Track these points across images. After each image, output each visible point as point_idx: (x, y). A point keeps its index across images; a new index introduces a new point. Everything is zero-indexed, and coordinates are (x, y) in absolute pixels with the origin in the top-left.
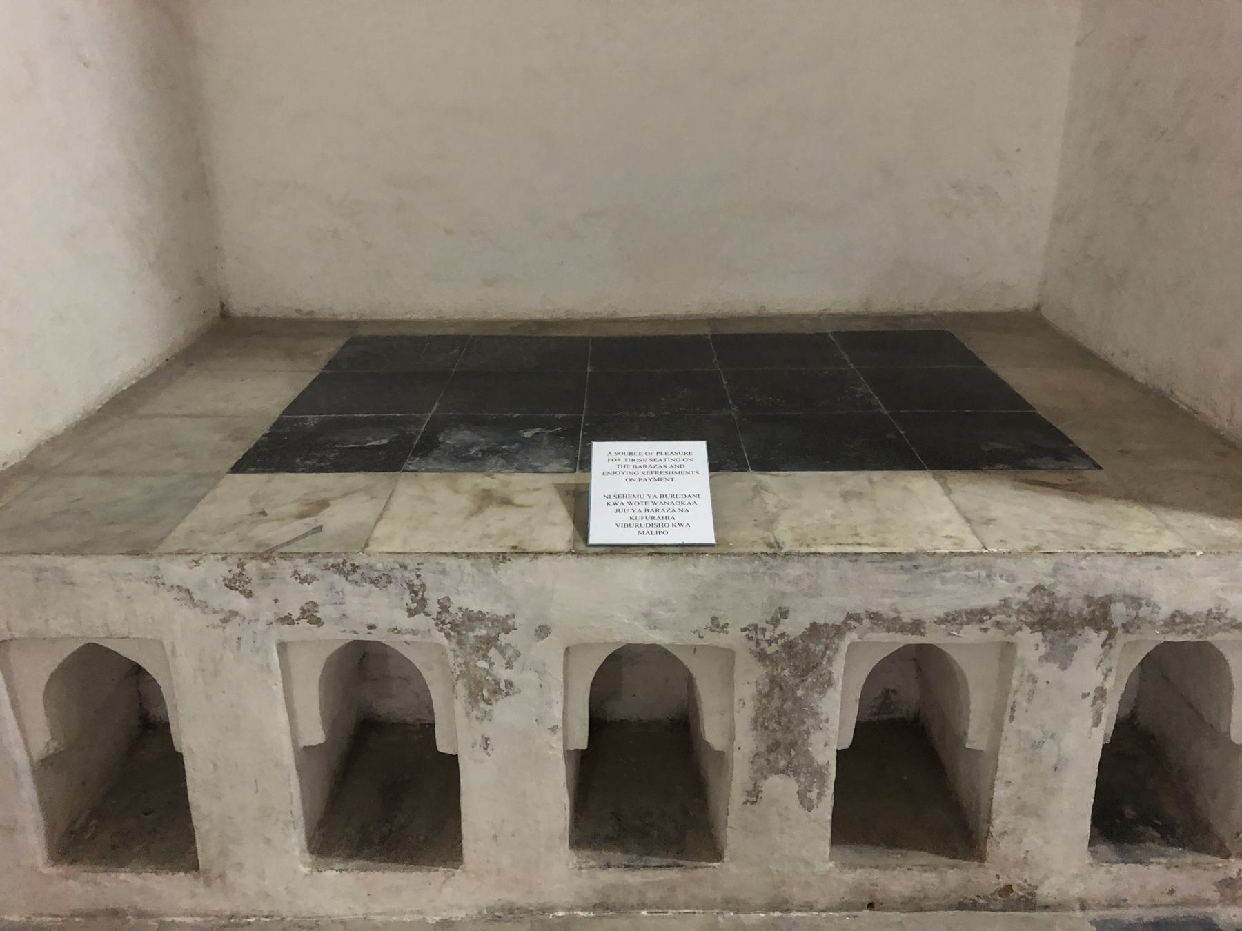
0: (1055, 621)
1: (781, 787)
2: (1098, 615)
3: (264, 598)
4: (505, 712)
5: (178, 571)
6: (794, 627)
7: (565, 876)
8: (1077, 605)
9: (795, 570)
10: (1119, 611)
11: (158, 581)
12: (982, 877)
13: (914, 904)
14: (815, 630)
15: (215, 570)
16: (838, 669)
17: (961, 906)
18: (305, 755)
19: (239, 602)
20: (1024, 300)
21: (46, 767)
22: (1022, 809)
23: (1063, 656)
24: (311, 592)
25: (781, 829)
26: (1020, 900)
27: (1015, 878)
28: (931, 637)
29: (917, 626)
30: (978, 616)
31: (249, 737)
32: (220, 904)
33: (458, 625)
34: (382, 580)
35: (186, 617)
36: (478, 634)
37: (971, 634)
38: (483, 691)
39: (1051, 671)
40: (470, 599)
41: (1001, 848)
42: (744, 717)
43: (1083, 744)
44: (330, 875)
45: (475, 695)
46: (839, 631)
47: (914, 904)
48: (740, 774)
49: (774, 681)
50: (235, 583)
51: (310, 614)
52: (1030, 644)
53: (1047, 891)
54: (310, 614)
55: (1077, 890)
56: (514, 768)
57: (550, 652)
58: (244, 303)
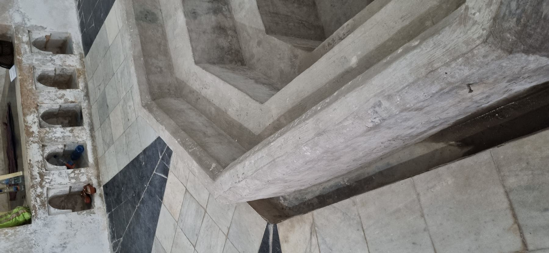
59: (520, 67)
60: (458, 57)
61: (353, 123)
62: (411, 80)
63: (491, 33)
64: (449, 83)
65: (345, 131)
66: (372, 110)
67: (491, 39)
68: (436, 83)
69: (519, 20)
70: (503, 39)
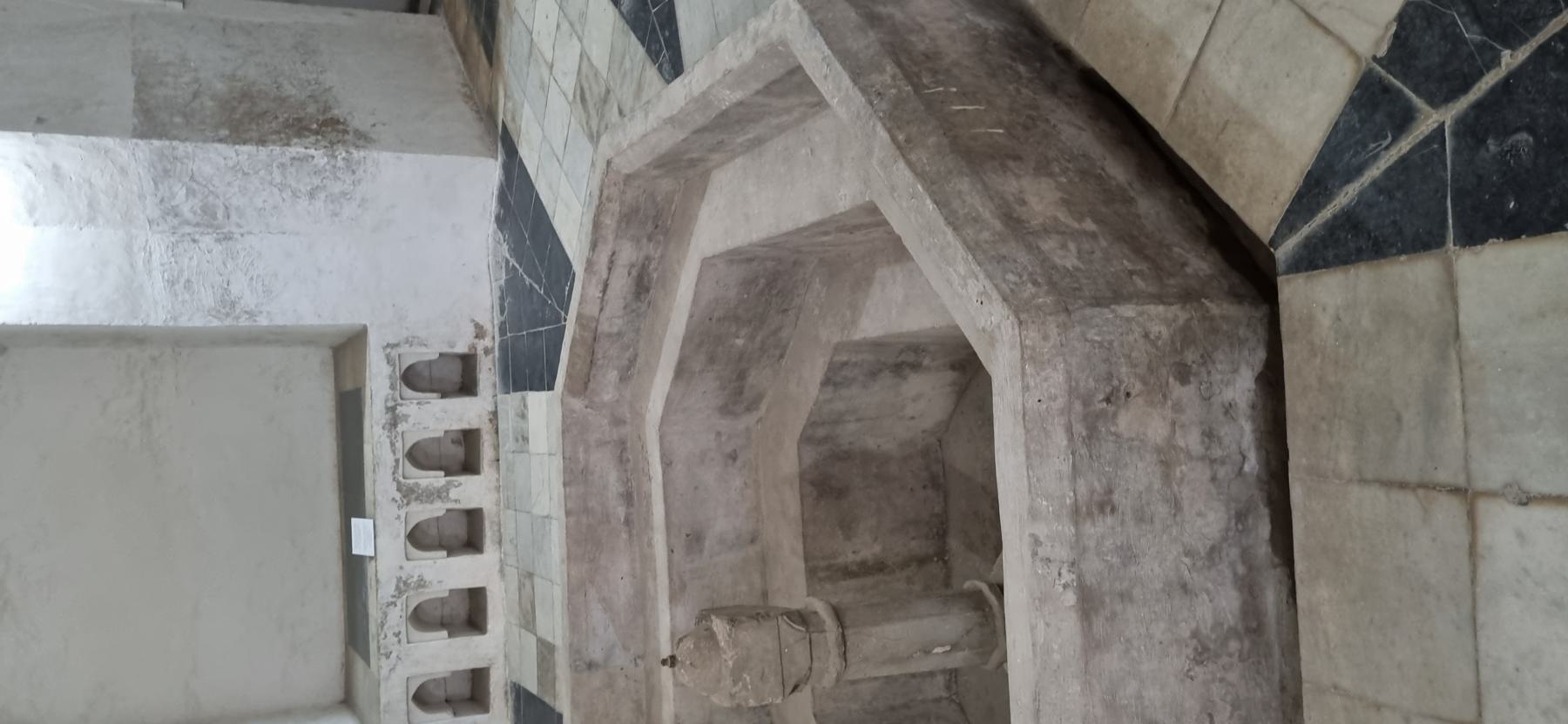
1: (453, 494)
2: (392, 409)
3: (392, 648)
4: (427, 578)
5: (384, 672)
6: (398, 496)
7: (490, 555)
8: (389, 416)
9: (379, 497)
10: (390, 404)
11: (387, 678)
13: (497, 447)
14: (399, 490)
15: (384, 661)
16: (411, 482)
18: (450, 636)
19: (394, 655)
21: (455, 714)
22: (461, 420)
23: (406, 417)
24: (390, 635)
25: (471, 491)
27: (486, 418)
28: (400, 455)
29: (397, 461)
30: (392, 444)
31: (443, 655)
32: (501, 660)
33: (400, 591)
34: (385, 614)
35: (399, 669)
36: (402, 586)
37: (399, 445)
38: (421, 583)
39: (411, 421)
40: (391, 589)
41: (475, 426)
42: (428, 506)
44: (489, 627)
45: (423, 586)
46: (399, 483)
47: (497, 447)
48: (450, 506)
49: (416, 499)
50: (388, 656)
51: (397, 635)
52: (400, 428)
53: (491, 408)
54: (397, 635)
56: (450, 573)
57: (408, 565)
58: (338, 694)
59: (1142, 341)
60: (1023, 369)
61: (1048, 625)
62: (1023, 458)
63: (1016, 313)
64: (1062, 412)
65: (1057, 657)
66: (1039, 564)
67: (1023, 316)
68: (1049, 427)
69: (1035, 283)
70: (1039, 308)
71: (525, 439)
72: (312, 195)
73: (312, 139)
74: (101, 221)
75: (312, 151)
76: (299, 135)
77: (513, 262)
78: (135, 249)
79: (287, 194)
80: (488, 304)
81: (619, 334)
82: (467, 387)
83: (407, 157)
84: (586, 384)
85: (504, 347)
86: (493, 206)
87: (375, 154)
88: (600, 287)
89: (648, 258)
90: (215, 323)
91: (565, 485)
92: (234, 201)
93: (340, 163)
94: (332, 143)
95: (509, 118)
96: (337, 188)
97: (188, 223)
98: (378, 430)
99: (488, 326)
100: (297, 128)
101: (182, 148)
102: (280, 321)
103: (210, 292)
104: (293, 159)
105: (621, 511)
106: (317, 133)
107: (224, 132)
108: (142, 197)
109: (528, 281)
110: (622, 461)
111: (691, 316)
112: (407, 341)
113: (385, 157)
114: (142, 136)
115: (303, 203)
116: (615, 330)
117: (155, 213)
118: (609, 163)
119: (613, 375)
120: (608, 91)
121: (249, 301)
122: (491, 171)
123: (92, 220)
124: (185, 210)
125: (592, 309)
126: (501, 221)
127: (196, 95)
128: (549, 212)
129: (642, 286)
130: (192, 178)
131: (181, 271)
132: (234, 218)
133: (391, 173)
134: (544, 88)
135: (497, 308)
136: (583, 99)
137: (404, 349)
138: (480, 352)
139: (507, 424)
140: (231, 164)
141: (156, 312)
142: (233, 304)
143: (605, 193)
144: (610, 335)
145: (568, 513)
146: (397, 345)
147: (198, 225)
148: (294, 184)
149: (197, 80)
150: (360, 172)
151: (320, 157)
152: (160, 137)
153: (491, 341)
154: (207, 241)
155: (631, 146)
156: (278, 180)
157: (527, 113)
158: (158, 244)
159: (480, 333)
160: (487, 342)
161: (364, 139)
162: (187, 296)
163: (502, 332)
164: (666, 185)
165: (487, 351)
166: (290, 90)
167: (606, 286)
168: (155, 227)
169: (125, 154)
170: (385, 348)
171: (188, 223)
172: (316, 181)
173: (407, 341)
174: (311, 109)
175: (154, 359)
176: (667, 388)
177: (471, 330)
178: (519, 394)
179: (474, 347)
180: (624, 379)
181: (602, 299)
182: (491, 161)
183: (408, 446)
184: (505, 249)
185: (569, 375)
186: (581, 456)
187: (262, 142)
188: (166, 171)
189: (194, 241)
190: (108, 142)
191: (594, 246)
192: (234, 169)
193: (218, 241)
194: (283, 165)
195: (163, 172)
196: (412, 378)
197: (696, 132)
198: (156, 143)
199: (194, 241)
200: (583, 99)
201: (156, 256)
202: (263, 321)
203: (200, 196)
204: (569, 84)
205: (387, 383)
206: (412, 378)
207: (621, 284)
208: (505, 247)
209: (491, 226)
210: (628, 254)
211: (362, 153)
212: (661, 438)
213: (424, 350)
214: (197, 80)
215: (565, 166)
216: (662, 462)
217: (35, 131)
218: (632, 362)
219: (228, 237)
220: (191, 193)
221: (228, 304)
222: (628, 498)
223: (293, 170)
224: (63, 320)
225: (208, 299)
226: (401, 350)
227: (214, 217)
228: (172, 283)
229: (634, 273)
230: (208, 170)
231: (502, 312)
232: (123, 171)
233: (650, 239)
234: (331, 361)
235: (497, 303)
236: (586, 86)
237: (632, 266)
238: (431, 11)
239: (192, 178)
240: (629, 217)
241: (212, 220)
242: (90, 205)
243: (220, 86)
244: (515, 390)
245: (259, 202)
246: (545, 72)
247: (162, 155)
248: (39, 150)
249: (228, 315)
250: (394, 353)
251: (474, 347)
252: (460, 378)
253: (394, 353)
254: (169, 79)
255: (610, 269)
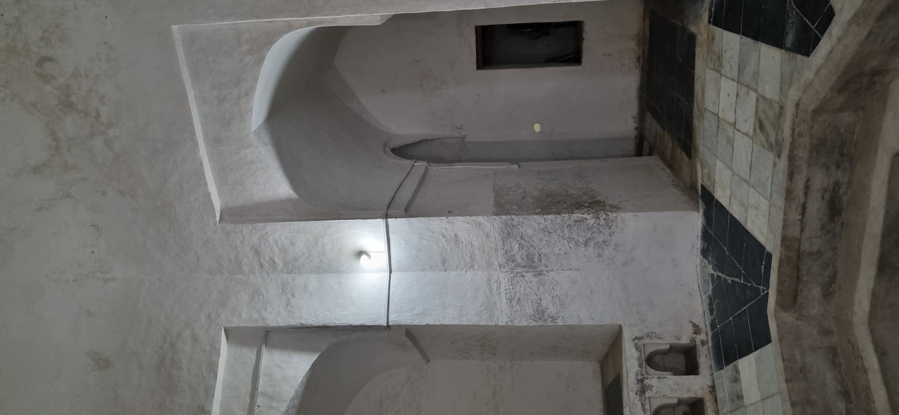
0: (643, 389)
2: (641, 381)
8: (639, 386)
10: (640, 377)
12: (708, 398)
17: (716, 401)
20: (598, 365)
22: (689, 391)
23: (650, 387)
26: (713, 389)
27: (707, 390)
30: (643, 405)
37: (647, 406)
39: (654, 389)
41: (699, 394)
43: (671, 380)
53: (710, 383)
55: (708, 377)
71: (740, 397)
72: (586, 244)
73: (586, 210)
74: (476, 267)
75: (586, 216)
76: (577, 209)
77: (716, 273)
78: (493, 281)
79: (572, 244)
80: (701, 311)
81: (819, 253)
82: (692, 369)
83: (641, 214)
84: (795, 298)
85: (715, 337)
86: (698, 244)
87: (622, 215)
88: (800, 210)
89: (837, 184)
90: (534, 324)
91: (787, 381)
92: (543, 250)
93: (602, 222)
94: (597, 211)
95: (706, 179)
96: (600, 238)
97: (519, 265)
98: (632, 395)
99: (702, 325)
100: (577, 206)
101: (517, 219)
102: (569, 322)
103: (530, 304)
104: (576, 221)
105: (841, 406)
106: (588, 207)
107: (538, 210)
108: (496, 250)
109: (729, 279)
110: (834, 363)
111: (887, 213)
112: (648, 336)
113: (628, 216)
114: (497, 215)
115: (582, 249)
116: (815, 248)
117: (502, 260)
118: (797, 105)
119: (816, 291)
120: (782, 108)
121: (552, 310)
122: (695, 220)
123: (472, 267)
124: (518, 257)
125: (795, 231)
126: (704, 252)
127: (524, 198)
128: (742, 222)
129: (835, 208)
130: (522, 237)
131: (516, 293)
132: (544, 261)
133: (633, 225)
134: (730, 142)
135: (708, 312)
136: (762, 127)
137: (647, 341)
138: (698, 343)
139: (723, 393)
140: (542, 226)
141: (502, 316)
142: (543, 312)
143: (797, 131)
144: (811, 254)
145: (793, 405)
146: (642, 338)
147: (524, 267)
148: (576, 238)
149: (525, 192)
150: (614, 228)
151: (590, 219)
152: (506, 214)
153: (706, 335)
154: (529, 276)
155: (817, 73)
156: (567, 234)
157: (719, 165)
158: (503, 278)
159: (697, 330)
160: (702, 336)
161: (615, 208)
162: (518, 308)
163: (713, 326)
164: (847, 118)
165: (703, 343)
166: (571, 191)
167: (804, 209)
168: (502, 269)
169: (488, 225)
170: (634, 340)
171: (519, 265)
172: (589, 235)
173: (648, 336)
174: (585, 198)
175: (501, 368)
176: (871, 283)
177: (690, 328)
178: (731, 366)
179: (693, 340)
180: (827, 294)
181: (802, 220)
182: (695, 214)
183: (654, 407)
184: (710, 269)
185: (779, 293)
186: (798, 357)
187: (559, 213)
188: (509, 234)
189: (523, 276)
190: (481, 219)
191: (791, 176)
192: (544, 230)
193: (535, 276)
194: (570, 225)
195: (507, 234)
196: (652, 361)
197: (881, 17)
198: (504, 217)
199: (523, 276)
200: (762, 127)
201: (503, 285)
202: (560, 322)
203: (525, 248)
204: (748, 126)
205: (636, 363)
206: (652, 361)
207: (816, 207)
208: (710, 267)
209: (697, 258)
210: (820, 180)
211: (615, 215)
212: (872, 332)
213: (660, 341)
214: (525, 192)
215: (752, 182)
216: (876, 351)
217: (447, 217)
218: (833, 279)
219: (540, 273)
220: (521, 246)
221: (540, 312)
222: (846, 395)
223: (575, 228)
224: (455, 322)
225: (529, 309)
226: (644, 341)
227: (534, 262)
228: (510, 300)
229: (827, 196)
230: (530, 231)
231: (711, 314)
232: (488, 235)
233: (838, 166)
234: (598, 370)
235: (706, 307)
236: (762, 116)
237: (825, 191)
238: (650, 154)
239: (522, 237)
240: (819, 147)
241: (532, 264)
242: (471, 257)
243: (536, 193)
244: (727, 364)
245: (557, 250)
246: (730, 131)
247: (506, 225)
248: (448, 226)
249: (540, 319)
250: (640, 343)
251: (693, 340)
252: (685, 360)
253: (640, 343)
254: (511, 193)
255: (806, 194)
